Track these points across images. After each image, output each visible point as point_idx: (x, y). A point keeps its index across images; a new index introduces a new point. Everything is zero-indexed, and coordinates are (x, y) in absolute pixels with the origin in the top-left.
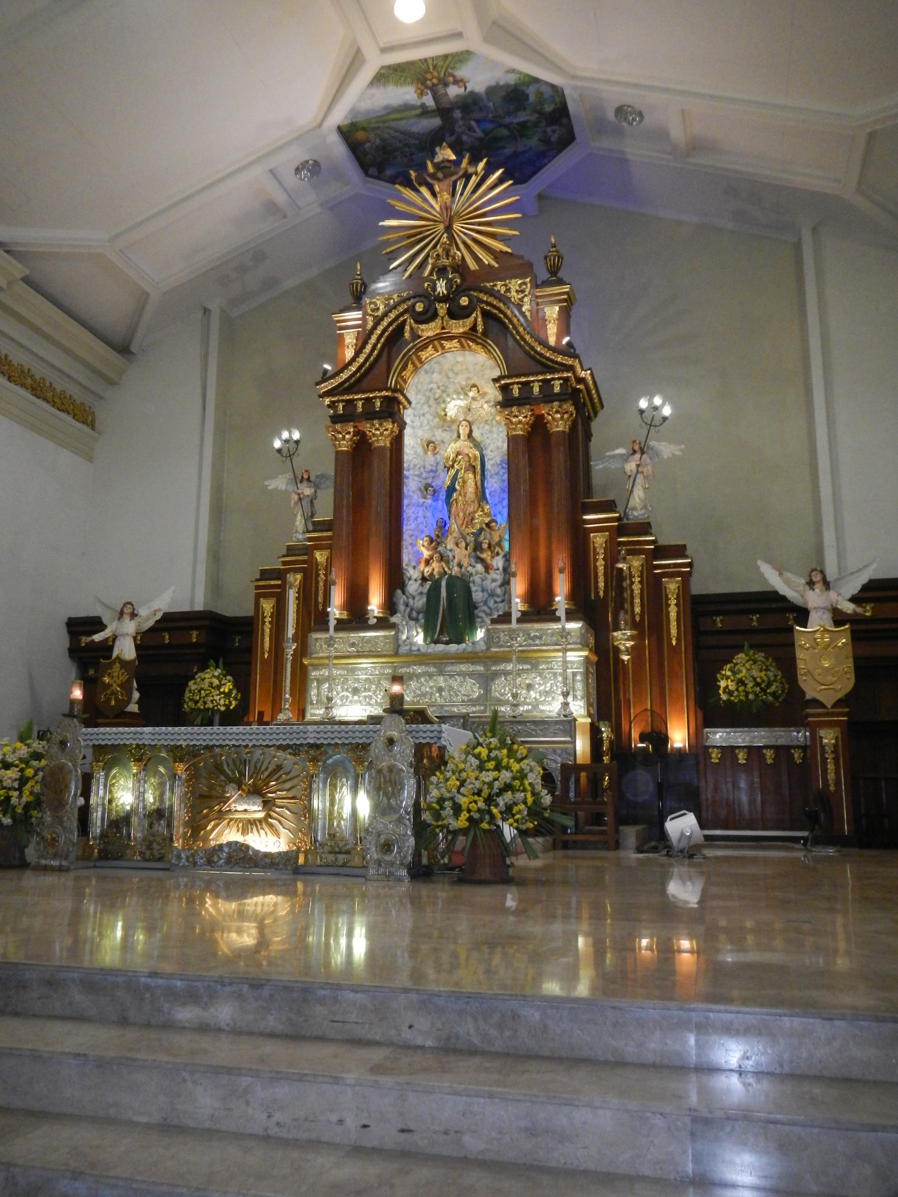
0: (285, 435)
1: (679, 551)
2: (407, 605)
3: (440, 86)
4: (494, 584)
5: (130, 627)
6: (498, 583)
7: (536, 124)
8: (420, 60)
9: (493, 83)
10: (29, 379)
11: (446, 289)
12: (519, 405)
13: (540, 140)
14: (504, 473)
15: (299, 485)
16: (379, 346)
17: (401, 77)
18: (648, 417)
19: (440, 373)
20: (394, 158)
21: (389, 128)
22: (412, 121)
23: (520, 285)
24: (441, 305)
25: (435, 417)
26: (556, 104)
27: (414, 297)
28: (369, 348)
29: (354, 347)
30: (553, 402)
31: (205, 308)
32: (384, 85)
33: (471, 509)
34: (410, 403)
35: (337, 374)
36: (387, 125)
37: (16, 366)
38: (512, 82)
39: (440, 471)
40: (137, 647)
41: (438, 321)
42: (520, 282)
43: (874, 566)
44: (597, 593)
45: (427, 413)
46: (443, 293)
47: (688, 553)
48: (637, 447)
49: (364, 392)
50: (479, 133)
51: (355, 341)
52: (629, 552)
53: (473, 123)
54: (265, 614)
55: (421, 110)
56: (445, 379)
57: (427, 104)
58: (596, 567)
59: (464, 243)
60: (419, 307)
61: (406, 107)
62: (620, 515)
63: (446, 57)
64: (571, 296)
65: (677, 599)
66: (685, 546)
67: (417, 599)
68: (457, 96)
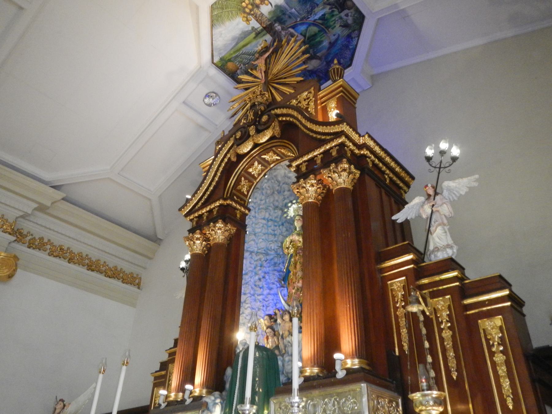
3: (255, 9)
7: (332, 15)
10: (87, 260)
18: (436, 162)
32: (223, 23)
34: (249, 210)
35: (191, 199)
36: (241, 52)
37: (76, 253)
41: (251, 139)
44: (401, 347)
45: (285, 222)
46: (251, 118)
48: (431, 192)
52: (433, 295)
53: (291, 30)
55: (254, 33)
57: (256, 27)
60: (239, 135)
61: (245, 34)
65: (502, 341)
68: (270, 13)
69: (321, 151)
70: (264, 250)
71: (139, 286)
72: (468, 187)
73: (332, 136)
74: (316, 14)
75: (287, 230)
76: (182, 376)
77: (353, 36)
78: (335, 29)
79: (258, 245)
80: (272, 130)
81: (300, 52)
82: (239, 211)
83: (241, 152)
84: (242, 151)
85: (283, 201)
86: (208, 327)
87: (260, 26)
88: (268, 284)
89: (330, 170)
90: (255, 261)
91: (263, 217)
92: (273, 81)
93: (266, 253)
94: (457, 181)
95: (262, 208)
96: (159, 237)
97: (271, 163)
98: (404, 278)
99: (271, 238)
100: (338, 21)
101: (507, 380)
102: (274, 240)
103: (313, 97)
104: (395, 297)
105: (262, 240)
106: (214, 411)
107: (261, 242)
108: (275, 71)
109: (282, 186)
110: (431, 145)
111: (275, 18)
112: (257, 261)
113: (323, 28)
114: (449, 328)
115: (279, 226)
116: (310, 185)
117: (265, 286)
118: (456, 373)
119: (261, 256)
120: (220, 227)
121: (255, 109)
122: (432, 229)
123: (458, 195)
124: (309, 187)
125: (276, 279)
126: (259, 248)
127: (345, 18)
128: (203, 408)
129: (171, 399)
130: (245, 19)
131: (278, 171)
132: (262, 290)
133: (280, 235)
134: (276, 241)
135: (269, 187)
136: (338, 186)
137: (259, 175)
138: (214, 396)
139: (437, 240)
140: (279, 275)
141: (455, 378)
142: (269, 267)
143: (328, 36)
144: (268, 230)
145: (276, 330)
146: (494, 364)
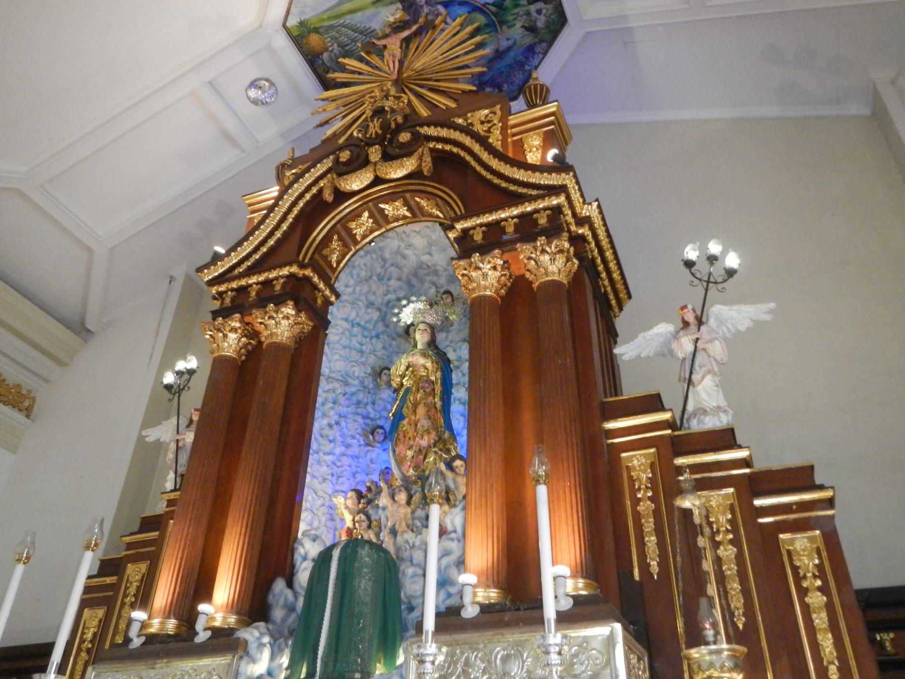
0: (181, 365)
11: (381, 128)
18: (703, 268)
23: (486, 116)
31: (171, 277)
33: (424, 443)
34: (338, 296)
36: (342, 21)
41: (370, 168)
44: (645, 567)
45: (383, 333)
46: (376, 133)
48: (690, 317)
58: (637, 516)
60: (345, 156)
62: (673, 417)
64: (559, 116)
66: (812, 468)
69: (515, 213)
70: (342, 376)
72: (752, 320)
73: (542, 192)
75: (384, 348)
76: (180, 586)
77: (537, 49)
78: (513, 29)
79: (332, 364)
80: (417, 161)
81: (472, 44)
82: (321, 294)
83: (348, 187)
84: (351, 187)
85: (385, 295)
86: (249, 498)
88: (343, 436)
89: (535, 248)
90: (324, 392)
91: (345, 316)
92: (410, 81)
93: (344, 380)
94: (735, 307)
95: (346, 301)
96: (90, 327)
97: (391, 220)
98: (653, 450)
99: (355, 356)
100: (521, 17)
101: (830, 636)
102: (360, 361)
103: (499, 122)
104: (634, 481)
105: (341, 356)
106: (260, 659)
107: (336, 360)
108: (418, 65)
109: (389, 269)
110: (695, 243)
112: (328, 391)
113: (494, 22)
114: (731, 542)
115: (371, 339)
116: (492, 267)
117: (339, 439)
118: (744, 619)
119: (336, 385)
120: (288, 313)
121: (384, 117)
122: (694, 377)
123: (733, 330)
124: (489, 270)
125: (359, 431)
126: (333, 369)
127: (535, 15)
128: (240, 653)
129: (152, 630)
131: (389, 240)
132: (332, 445)
133: (370, 353)
134: (363, 364)
135: (365, 265)
136: (547, 276)
137: (364, 237)
138: (257, 628)
139: (704, 395)
140: (364, 423)
141: (741, 626)
142: (348, 406)
143: (497, 38)
144: (350, 340)
145: (373, 518)
146: (807, 610)
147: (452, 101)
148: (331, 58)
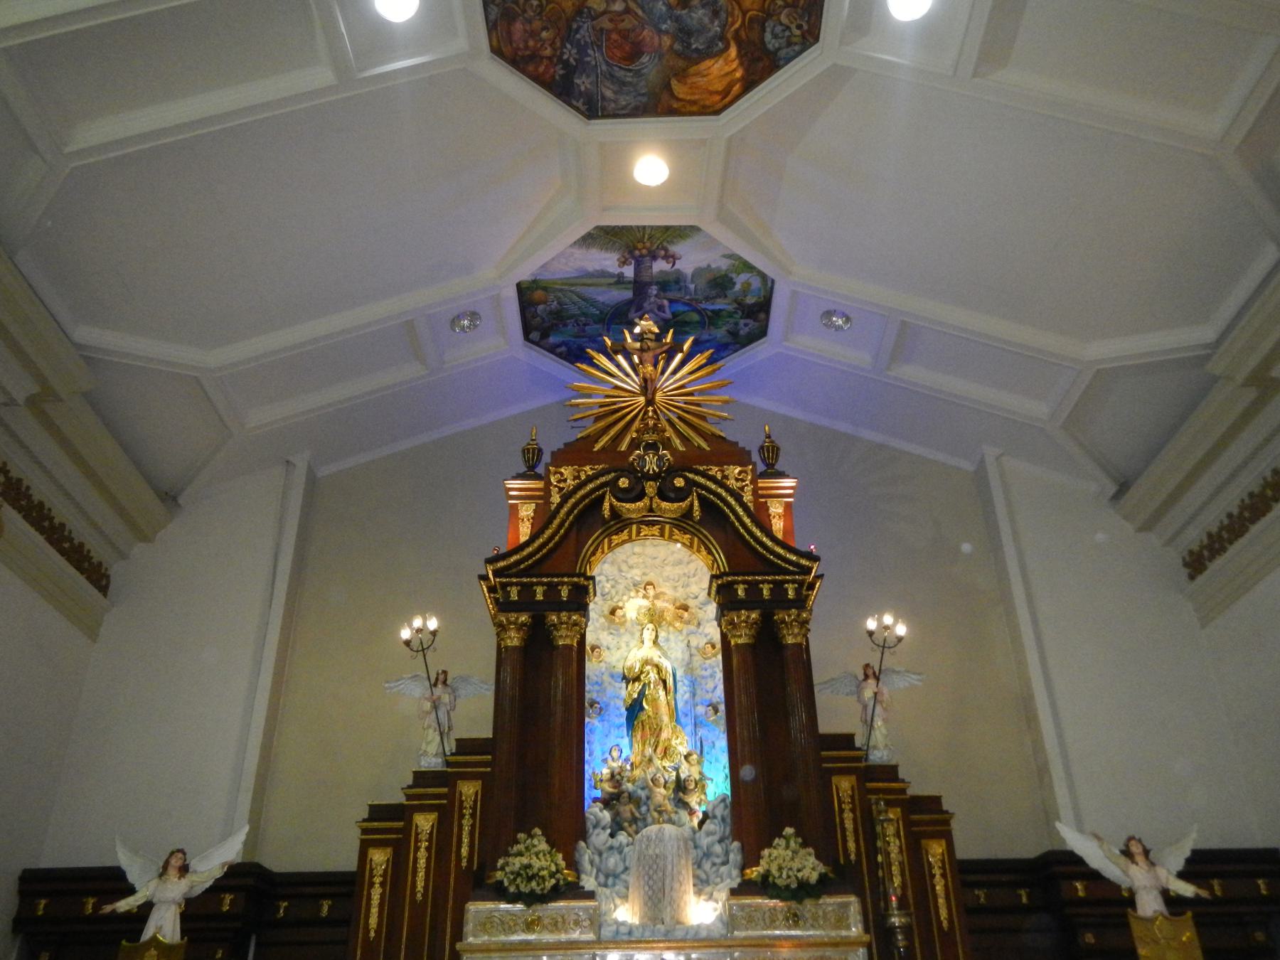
0: (418, 622)
1: (933, 803)
2: (592, 862)
3: (648, 258)
4: (710, 839)
5: (176, 889)
6: (716, 837)
7: (730, 315)
8: (638, 227)
9: (704, 264)
12: (747, 609)
13: (728, 332)
14: (686, 693)
15: (433, 689)
16: (566, 525)
17: (611, 240)
19: (612, 563)
20: (565, 325)
21: (571, 291)
22: (600, 289)
23: (740, 473)
24: (651, 483)
25: (600, 616)
26: (760, 298)
27: (615, 472)
28: (556, 522)
29: (531, 520)
30: (790, 608)
31: (288, 462)
36: (573, 288)
38: (724, 268)
39: (606, 684)
40: (185, 918)
41: (646, 501)
42: (738, 469)
43: (1194, 835)
47: (945, 808)
49: (547, 576)
50: (668, 315)
51: (532, 514)
53: (666, 302)
54: (375, 872)
55: (615, 279)
56: (616, 572)
57: (625, 275)
59: (669, 421)
60: (624, 483)
61: (603, 274)
63: (667, 228)
65: (943, 868)
67: (605, 855)
68: (661, 272)
71: (104, 590)
74: (713, 304)
78: (719, 330)
87: (633, 276)
111: (660, 280)
130: (623, 260)
147: (703, 440)
148: (545, 310)
